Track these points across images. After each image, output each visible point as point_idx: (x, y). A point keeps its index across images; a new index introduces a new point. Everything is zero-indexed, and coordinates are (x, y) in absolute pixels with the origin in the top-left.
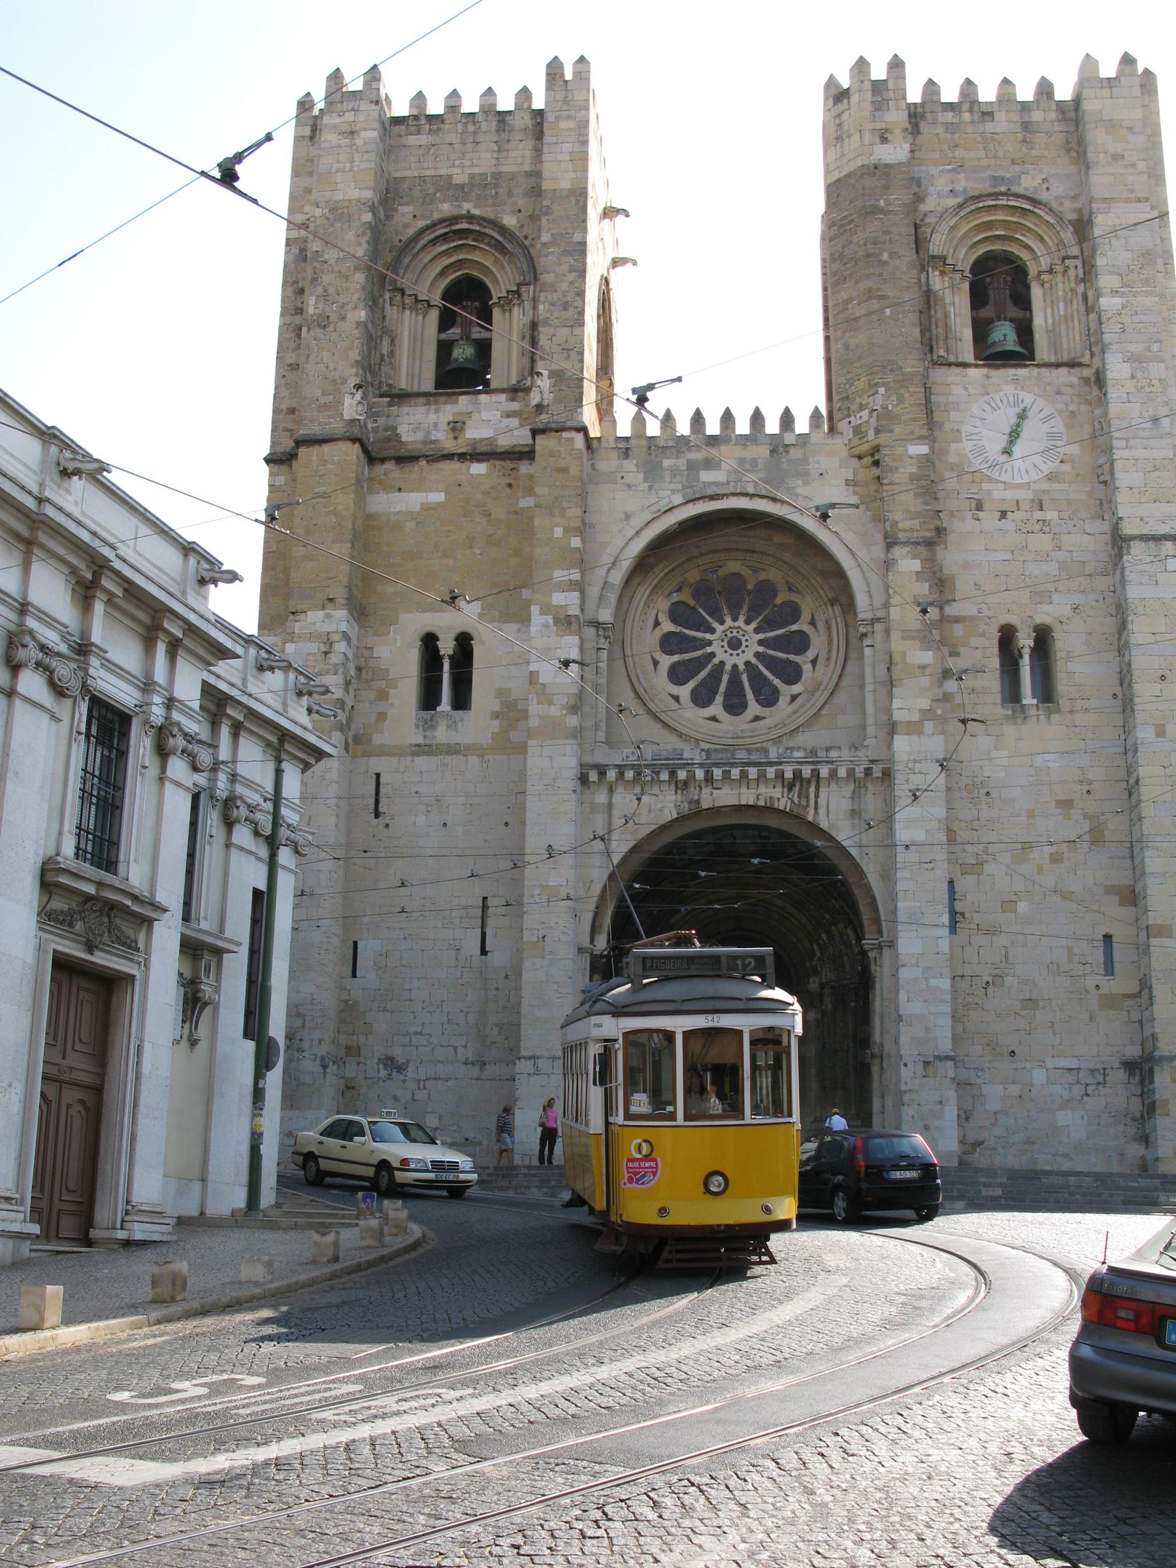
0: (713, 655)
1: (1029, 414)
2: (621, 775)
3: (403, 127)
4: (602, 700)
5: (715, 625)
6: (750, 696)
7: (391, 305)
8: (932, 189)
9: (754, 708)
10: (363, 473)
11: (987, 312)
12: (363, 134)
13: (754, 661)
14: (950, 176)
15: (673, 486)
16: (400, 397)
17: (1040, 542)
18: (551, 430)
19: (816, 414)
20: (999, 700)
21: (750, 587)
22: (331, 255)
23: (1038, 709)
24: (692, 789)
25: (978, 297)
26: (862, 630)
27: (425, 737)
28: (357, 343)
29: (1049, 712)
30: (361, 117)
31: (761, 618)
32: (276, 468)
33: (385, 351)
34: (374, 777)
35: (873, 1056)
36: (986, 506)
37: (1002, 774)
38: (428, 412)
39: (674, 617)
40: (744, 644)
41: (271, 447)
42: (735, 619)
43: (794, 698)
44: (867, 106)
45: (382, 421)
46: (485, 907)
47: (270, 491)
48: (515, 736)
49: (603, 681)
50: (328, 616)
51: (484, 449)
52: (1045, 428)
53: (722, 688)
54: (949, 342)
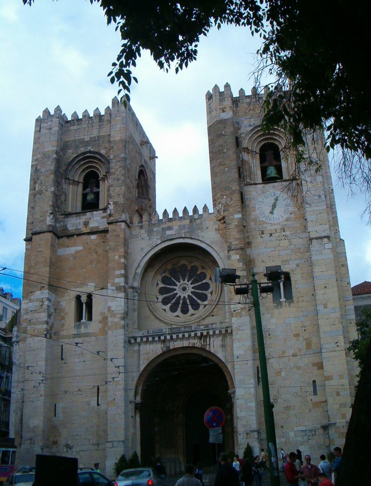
0: (177, 294)
1: (279, 199)
2: (142, 339)
3: (69, 124)
4: (136, 314)
5: (177, 283)
6: (190, 307)
7: (65, 184)
8: (243, 125)
9: (191, 311)
10: (55, 242)
11: (266, 164)
12: (53, 129)
13: (191, 294)
14: (249, 120)
15: (157, 237)
16: (68, 215)
17: (285, 243)
18: (114, 223)
19: (205, 208)
20: (272, 300)
21: (189, 269)
22: (43, 170)
23: (286, 302)
24: (166, 343)
25: (263, 160)
27: (77, 331)
28: (51, 199)
29: (290, 303)
30: (53, 123)
31: (192, 280)
32: (28, 243)
33: (63, 200)
34: (61, 346)
36: (264, 233)
37: (274, 327)
38: (77, 219)
39: (164, 282)
40: (187, 289)
41: (26, 236)
42: (184, 280)
43: (205, 306)
44: (218, 101)
45: (62, 223)
46: (98, 389)
47: (26, 251)
49: (136, 307)
50: (42, 293)
51: (95, 230)
52: (285, 203)
54: (252, 176)
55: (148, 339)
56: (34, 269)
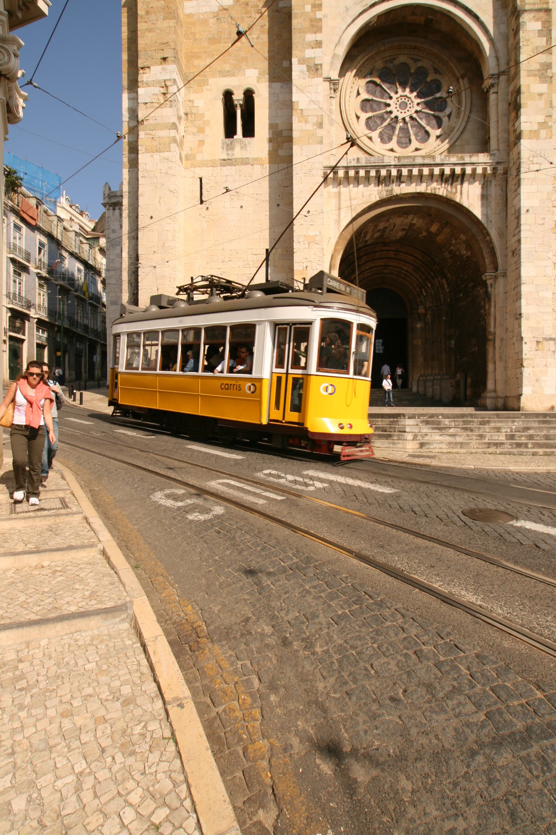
0: (391, 112)
5: (392, 94)
6: (413, 138)
9: (415, 144)
21: (412, 71)
26: (491, 81)
27: (228, 155)
35: (490, 340)
40: (409, 106)
43: (438, 137)
48: (282, 153)
53: (397, 132)
55: (357, 173)
56: (146, 22)
